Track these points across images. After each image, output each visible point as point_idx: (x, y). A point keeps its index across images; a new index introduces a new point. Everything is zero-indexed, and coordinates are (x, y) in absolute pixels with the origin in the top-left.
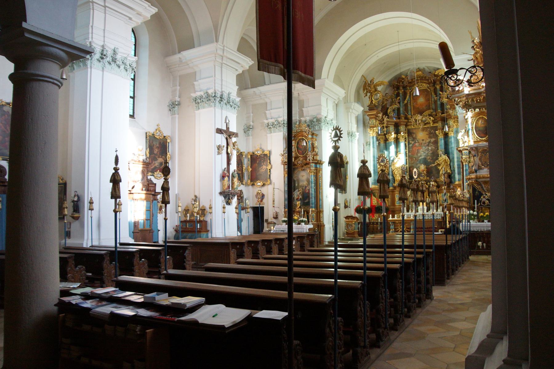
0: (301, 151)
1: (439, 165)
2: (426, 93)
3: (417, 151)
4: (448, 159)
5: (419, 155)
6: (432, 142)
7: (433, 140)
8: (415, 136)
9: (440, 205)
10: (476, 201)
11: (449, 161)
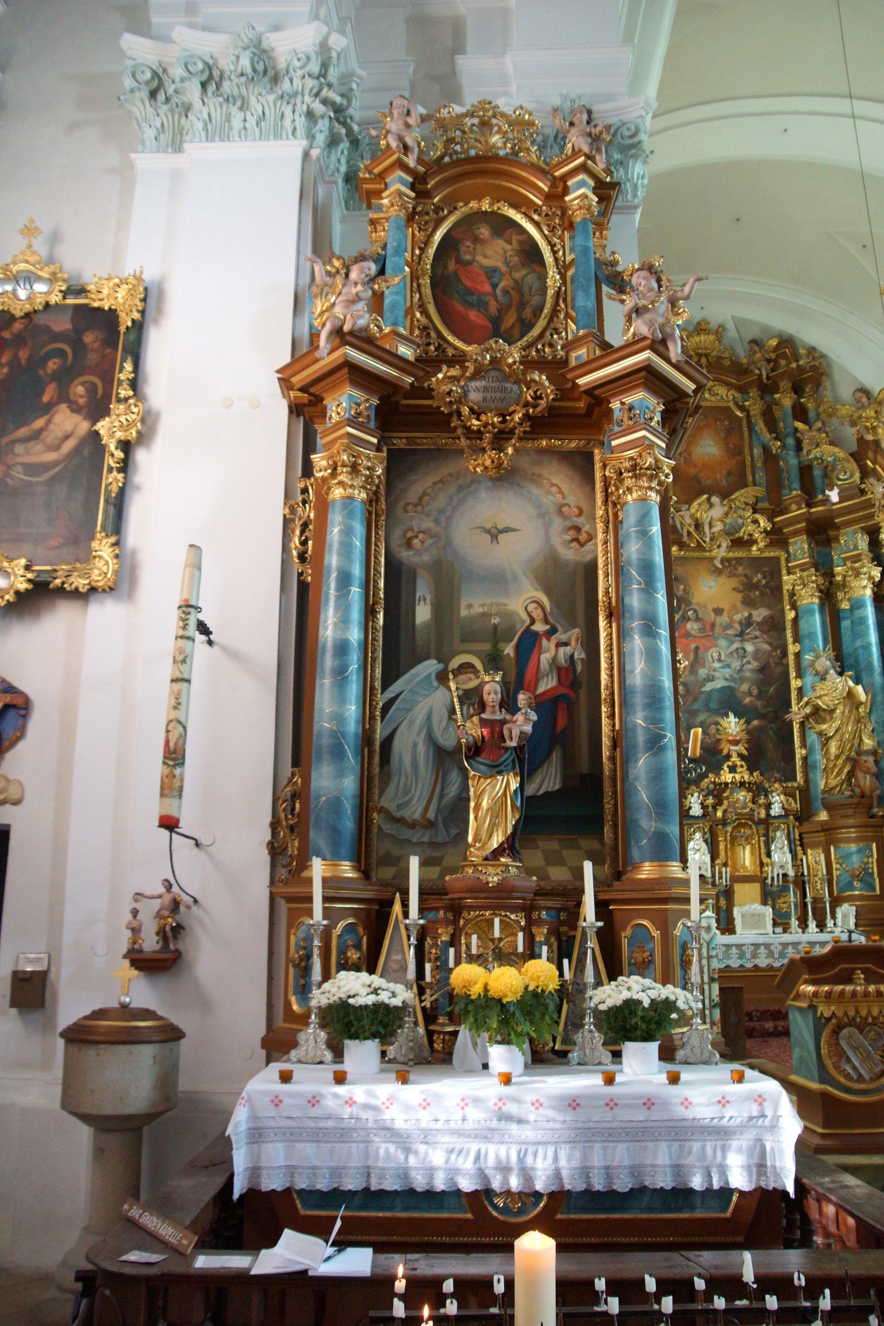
0: (473, 315)
2: (726, 423)
5: (702, 672)
6: (758, 623)
7: (760, 614)
8: (684, 590)
9: (836, 902)
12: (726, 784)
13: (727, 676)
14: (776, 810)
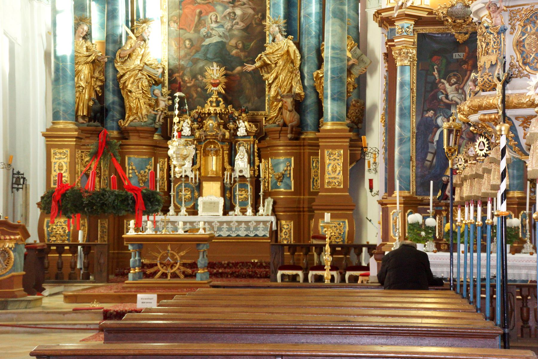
1: (266, 66)
3: (197, 18)
4: (297, 52)
5: (203, 31)
9: (267, 194)
10: (432, 182)
11: (299, 58)
12: (205, 114)
13: (221, 34)
14: (241, 132)
